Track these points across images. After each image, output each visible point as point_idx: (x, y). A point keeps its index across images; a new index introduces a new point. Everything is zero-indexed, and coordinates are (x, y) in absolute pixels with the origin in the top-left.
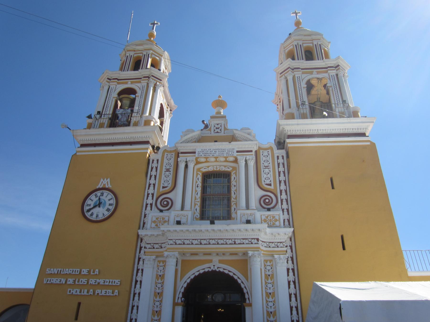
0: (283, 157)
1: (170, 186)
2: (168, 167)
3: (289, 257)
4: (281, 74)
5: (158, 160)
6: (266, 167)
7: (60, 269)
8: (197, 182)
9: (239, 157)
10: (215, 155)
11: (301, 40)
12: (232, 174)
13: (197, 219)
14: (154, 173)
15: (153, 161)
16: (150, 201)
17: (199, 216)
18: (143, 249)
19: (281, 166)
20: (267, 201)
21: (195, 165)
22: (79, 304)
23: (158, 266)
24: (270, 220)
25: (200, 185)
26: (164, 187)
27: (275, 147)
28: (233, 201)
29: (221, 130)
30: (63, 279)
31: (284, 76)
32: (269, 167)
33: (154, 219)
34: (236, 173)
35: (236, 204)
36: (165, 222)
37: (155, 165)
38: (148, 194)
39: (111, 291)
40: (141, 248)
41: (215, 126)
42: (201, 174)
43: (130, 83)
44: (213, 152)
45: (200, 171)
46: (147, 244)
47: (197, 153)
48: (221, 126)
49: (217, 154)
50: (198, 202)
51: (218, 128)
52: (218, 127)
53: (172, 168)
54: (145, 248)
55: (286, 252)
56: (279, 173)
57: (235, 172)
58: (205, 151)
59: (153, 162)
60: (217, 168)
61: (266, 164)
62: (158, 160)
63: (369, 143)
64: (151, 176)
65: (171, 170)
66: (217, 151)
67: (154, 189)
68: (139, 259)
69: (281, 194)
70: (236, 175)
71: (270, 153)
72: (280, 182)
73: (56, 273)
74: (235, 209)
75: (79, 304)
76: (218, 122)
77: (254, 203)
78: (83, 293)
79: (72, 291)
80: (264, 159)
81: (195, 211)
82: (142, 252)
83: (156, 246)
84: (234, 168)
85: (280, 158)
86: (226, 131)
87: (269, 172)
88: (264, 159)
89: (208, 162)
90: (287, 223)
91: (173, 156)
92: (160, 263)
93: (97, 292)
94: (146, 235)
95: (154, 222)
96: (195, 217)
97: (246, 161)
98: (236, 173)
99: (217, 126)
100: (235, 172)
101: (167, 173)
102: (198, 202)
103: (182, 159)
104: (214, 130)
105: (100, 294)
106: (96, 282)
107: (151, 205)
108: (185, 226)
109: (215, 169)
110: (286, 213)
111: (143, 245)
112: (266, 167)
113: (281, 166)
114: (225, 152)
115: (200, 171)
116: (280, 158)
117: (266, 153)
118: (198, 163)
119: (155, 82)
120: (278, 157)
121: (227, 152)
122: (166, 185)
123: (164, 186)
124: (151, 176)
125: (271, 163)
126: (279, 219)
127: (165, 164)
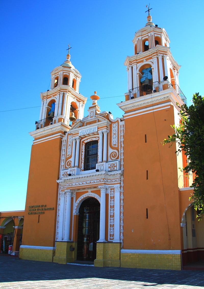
10: (87, 133)
11: (140, 36)
13: (82, 170)
17: (83, 168)
20: (113, 155)
26: (68, 155)
33: (63, 173)
42: (84, 144)
43: (52, 96)
47: (79, 133)
50: (83, 161)
60: (91, 139)
63: (169, 107)
71: (117, 125)
82: (60, 190)
85: (122, 126)
94: (60, 182)
95: (63, 175)
102: (83, 161)
108: (74, 176)
114: (92, 130)
115: (84, 143)
119: (63, 92)
122: (69, 154)
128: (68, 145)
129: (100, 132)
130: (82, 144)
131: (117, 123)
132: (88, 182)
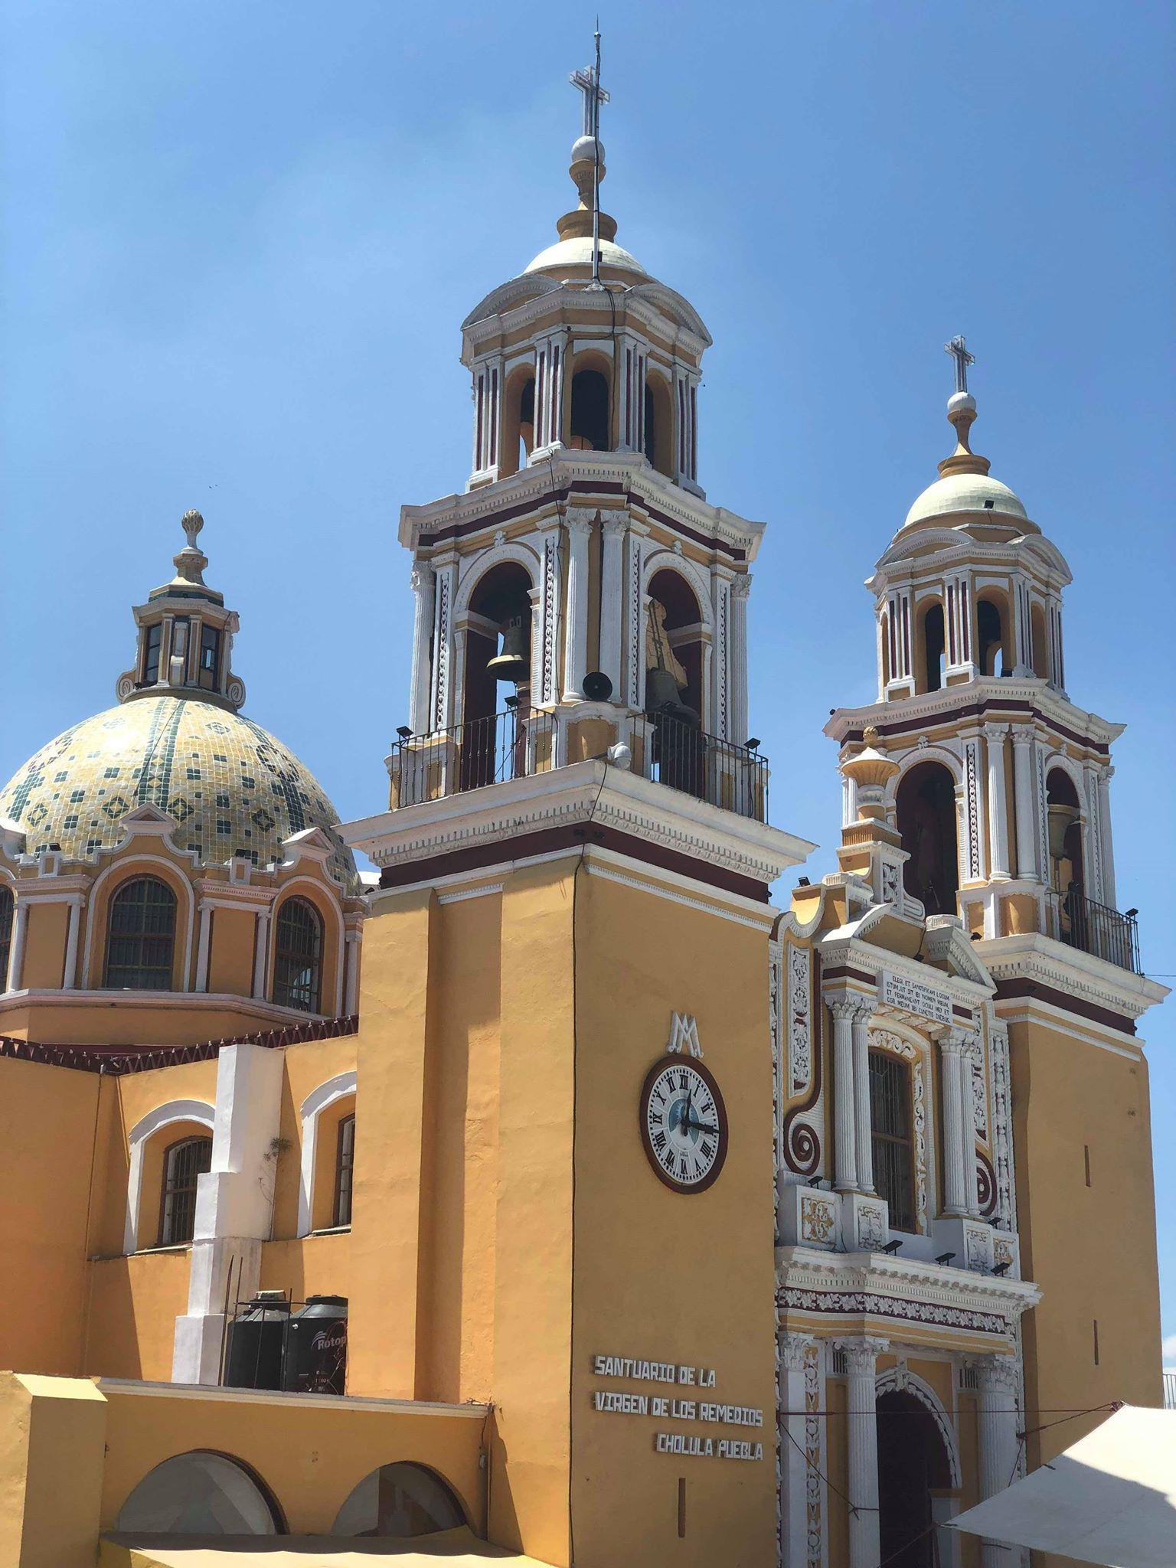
1: (808, 1080)
9: (955, 1033)
30: (641, 1399)
31: (1005, 727)
39: (748, 1446)
53: (808, 1010)
65: (807, 1019)
79: (668, 1443)
93: (720, 1449)
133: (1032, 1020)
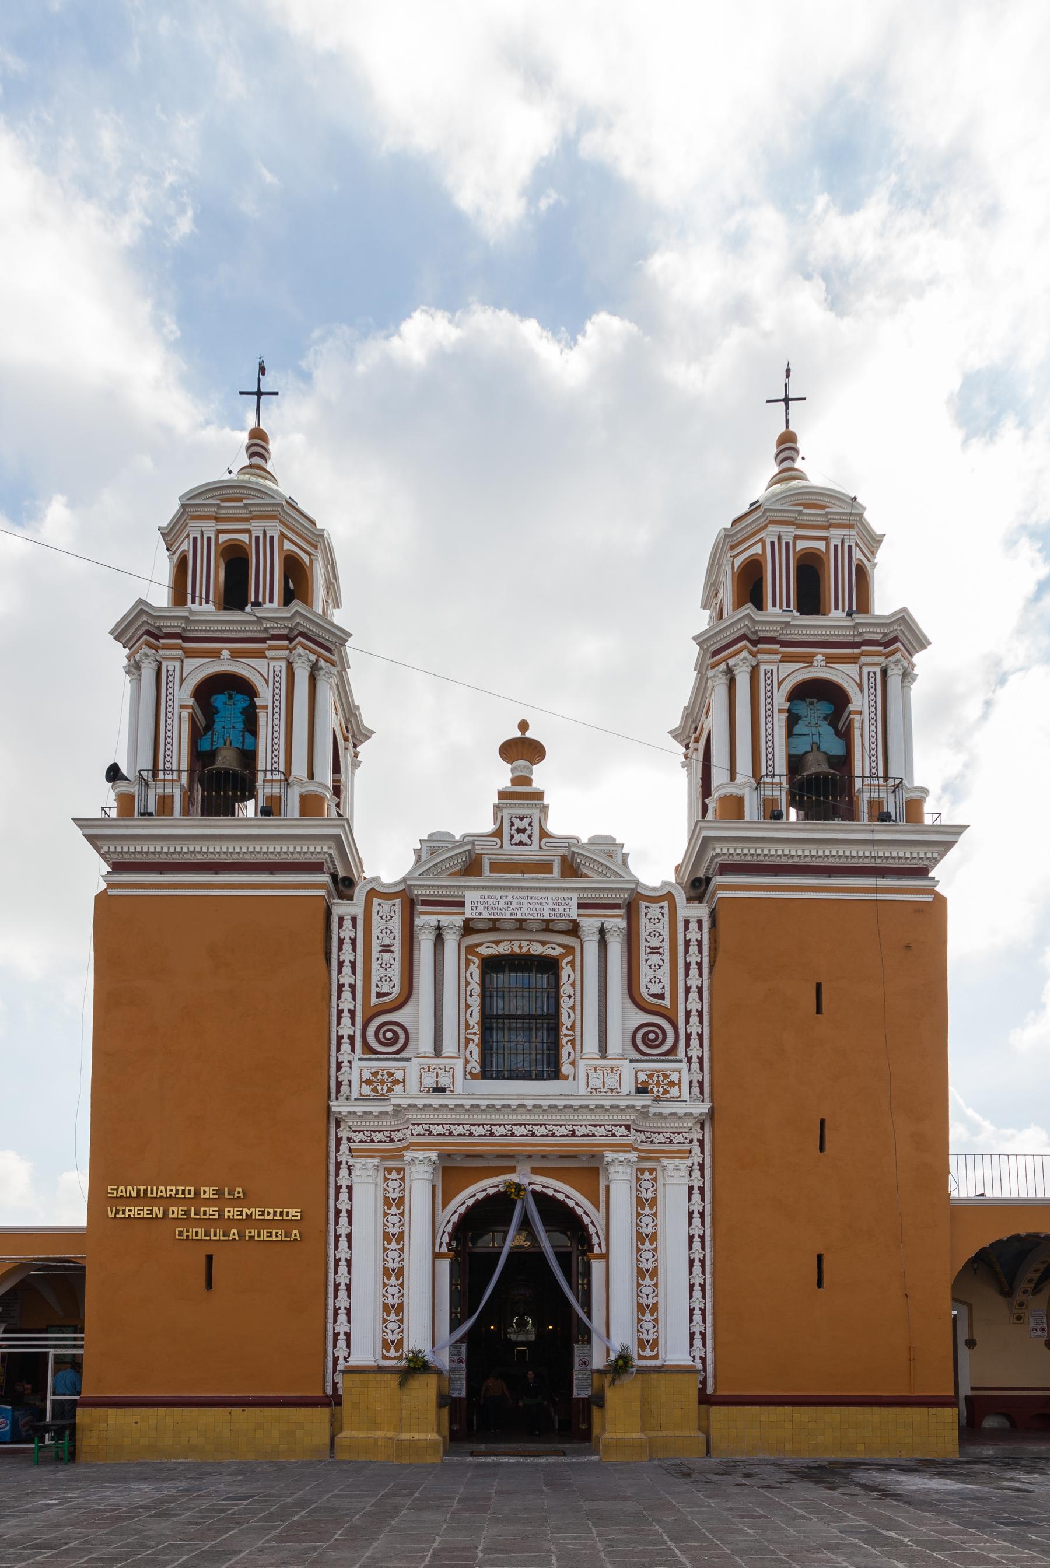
0: (700, 922)
1: (396, 991)
2: (386, 942)
3: (696, 1164)
4: (715, 654)
5: (354, 920)
6: (655, 950)
7: (142, 1188)
8: (468, 983)
9: (584, 922)
12: (564, 964)
13: (474, 1076)
14: (347, 956)
15: (341, 920)
16: (346, 1030)
18: (344, 1141)
19: (693, 948)
20: (652, 1036)
21: (463, 936)
22: (209, 1258)
23: (386, 1179)
24: (658, 1084)
25: (477, 990)
26: (379, 995)
27: (681, 897)
28: (566, 1035)
29: (530, 837)
30: (155, 1209)
31: (723, 666)
32: (661, 951)
34: (572, 963)
35: (573, 1042)
36: (397, 1082)
37: (347, 933)
38: (340, 1012)
40: (339, 1141)
41: (512, 824)
42: (477, 961)
44: (514, 905)
45: (477, 955)
46: (355, 1132)
48: (530, 824)
49: (525, 910)
50: (475, 1034)
51: (524, 831)
52: (522, 827)
54: (349, 1139)
55: (690, 1152)
56: (688, 966)
57: (570, 958)
58: (490, 901)
59: (340, 926)
61: (654, 942)
62: (354, 920)
64: (341, 964)
66: (525, 902)
67: (354, 999)
68: (338, 1165)
69: (687, 1022)
70: (574, 970)
71: (666, 911)
72: (688, 990)
73: (134, 1195)
74: (569, 1054)
75: (209, 1258)
76: (521, 812)
77: (616, 1043)
78: (215, 1235)
79: (185, 1234)
80: (651, 927)
81: (468, 1056)
82: (344, 1148)
83: (379, 1137)
84: (570, 950)
85: (693, 926)
86: (544, 840)
87: (661, 963)
88: (651, 927)
89: (499, 930)
90: (696, 1090)
91: (398, 909)
92: (390, 1174)
96: (468, 1070)
97: (602, 931)
98: (572, 963)
99: (518, 824)
100: (570, 958)
101: (386, 956)
102: (475, 1034)
103: (426, 920)
104: (512, 837)
105: (256, 1238)
106: (241, 1215)
107: (352, 1038)
109: (517, 950)
110: (695, 1066)
111: (344, 1134)
112: (655, 950)
113: (693, 948)
114: (547, 908)
115: (477, 955)
116: (693, 926)
117: (654, 910)
118: (468, 928)
120: (687, 923)
121: (551, 906)
122: (385, 990)
123: (379, 990)
124: (341, 964)
125: (667, 940)
126: (680, 1080)
127: (375, 931)
128: (375, 948)
129: (590, 924)
130: (467, 958)
131: (665, 904)
132: (499, 1131)
133: (721, 894)
